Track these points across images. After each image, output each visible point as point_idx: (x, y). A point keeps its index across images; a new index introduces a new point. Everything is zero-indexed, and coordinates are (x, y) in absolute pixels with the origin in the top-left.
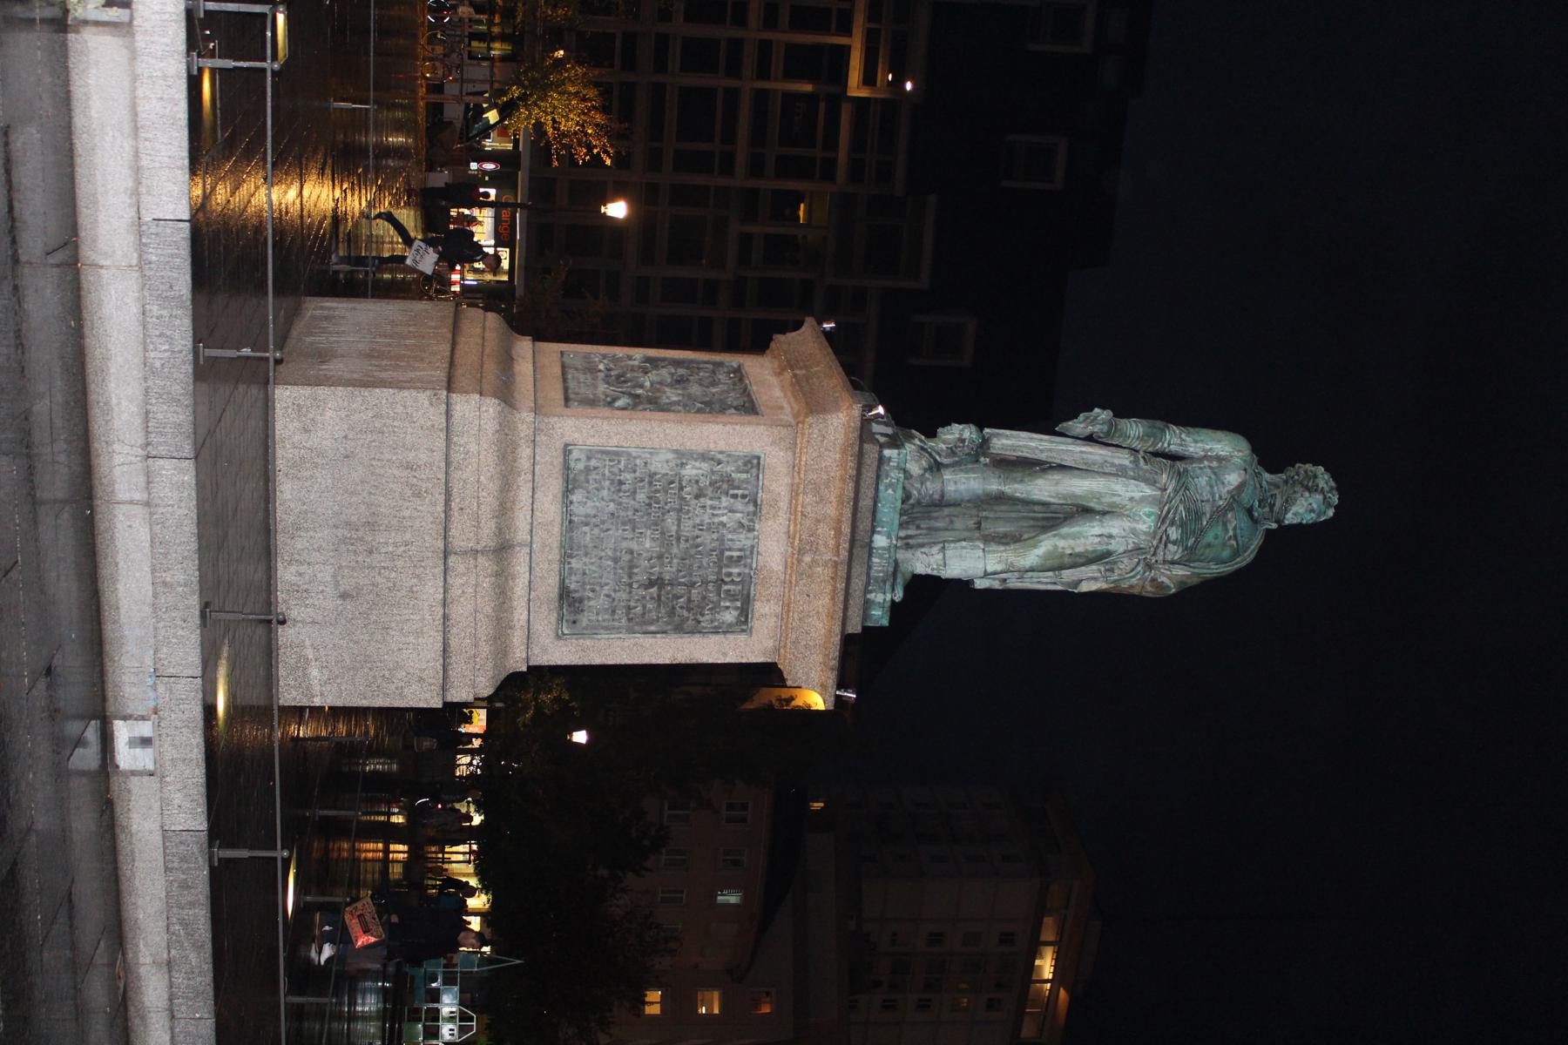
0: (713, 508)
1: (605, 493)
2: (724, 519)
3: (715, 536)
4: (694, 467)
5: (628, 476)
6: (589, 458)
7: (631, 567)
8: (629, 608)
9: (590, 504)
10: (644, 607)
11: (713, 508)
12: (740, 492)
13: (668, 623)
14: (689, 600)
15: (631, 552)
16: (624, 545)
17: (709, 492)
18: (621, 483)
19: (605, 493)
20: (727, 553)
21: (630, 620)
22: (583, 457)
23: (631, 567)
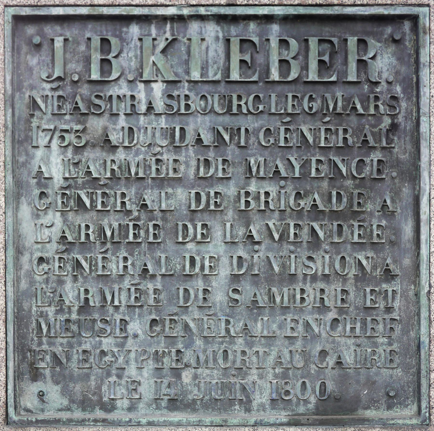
0: (133, 113)
1: (107, 343)
2: (158, 88)
3: (196, 104)
4: (47, 160)
5: (71, 293)
6: (36, 375)
7: (270, 278)
8: (362, 276)
9: (132, 371)
10: (360, 246)
11: (133, 113)
12: (96, 57)
13: (396, 195)
14: (345, 149)
15: (235, 278)
16: (219, 297)
17: (96, 124)
18: (85, 308)
19: (107, 343)
20: (235, 76)
21: (389, 275)
22: (35, 388)
23: (270, 278)
